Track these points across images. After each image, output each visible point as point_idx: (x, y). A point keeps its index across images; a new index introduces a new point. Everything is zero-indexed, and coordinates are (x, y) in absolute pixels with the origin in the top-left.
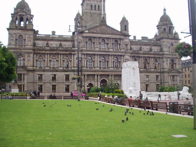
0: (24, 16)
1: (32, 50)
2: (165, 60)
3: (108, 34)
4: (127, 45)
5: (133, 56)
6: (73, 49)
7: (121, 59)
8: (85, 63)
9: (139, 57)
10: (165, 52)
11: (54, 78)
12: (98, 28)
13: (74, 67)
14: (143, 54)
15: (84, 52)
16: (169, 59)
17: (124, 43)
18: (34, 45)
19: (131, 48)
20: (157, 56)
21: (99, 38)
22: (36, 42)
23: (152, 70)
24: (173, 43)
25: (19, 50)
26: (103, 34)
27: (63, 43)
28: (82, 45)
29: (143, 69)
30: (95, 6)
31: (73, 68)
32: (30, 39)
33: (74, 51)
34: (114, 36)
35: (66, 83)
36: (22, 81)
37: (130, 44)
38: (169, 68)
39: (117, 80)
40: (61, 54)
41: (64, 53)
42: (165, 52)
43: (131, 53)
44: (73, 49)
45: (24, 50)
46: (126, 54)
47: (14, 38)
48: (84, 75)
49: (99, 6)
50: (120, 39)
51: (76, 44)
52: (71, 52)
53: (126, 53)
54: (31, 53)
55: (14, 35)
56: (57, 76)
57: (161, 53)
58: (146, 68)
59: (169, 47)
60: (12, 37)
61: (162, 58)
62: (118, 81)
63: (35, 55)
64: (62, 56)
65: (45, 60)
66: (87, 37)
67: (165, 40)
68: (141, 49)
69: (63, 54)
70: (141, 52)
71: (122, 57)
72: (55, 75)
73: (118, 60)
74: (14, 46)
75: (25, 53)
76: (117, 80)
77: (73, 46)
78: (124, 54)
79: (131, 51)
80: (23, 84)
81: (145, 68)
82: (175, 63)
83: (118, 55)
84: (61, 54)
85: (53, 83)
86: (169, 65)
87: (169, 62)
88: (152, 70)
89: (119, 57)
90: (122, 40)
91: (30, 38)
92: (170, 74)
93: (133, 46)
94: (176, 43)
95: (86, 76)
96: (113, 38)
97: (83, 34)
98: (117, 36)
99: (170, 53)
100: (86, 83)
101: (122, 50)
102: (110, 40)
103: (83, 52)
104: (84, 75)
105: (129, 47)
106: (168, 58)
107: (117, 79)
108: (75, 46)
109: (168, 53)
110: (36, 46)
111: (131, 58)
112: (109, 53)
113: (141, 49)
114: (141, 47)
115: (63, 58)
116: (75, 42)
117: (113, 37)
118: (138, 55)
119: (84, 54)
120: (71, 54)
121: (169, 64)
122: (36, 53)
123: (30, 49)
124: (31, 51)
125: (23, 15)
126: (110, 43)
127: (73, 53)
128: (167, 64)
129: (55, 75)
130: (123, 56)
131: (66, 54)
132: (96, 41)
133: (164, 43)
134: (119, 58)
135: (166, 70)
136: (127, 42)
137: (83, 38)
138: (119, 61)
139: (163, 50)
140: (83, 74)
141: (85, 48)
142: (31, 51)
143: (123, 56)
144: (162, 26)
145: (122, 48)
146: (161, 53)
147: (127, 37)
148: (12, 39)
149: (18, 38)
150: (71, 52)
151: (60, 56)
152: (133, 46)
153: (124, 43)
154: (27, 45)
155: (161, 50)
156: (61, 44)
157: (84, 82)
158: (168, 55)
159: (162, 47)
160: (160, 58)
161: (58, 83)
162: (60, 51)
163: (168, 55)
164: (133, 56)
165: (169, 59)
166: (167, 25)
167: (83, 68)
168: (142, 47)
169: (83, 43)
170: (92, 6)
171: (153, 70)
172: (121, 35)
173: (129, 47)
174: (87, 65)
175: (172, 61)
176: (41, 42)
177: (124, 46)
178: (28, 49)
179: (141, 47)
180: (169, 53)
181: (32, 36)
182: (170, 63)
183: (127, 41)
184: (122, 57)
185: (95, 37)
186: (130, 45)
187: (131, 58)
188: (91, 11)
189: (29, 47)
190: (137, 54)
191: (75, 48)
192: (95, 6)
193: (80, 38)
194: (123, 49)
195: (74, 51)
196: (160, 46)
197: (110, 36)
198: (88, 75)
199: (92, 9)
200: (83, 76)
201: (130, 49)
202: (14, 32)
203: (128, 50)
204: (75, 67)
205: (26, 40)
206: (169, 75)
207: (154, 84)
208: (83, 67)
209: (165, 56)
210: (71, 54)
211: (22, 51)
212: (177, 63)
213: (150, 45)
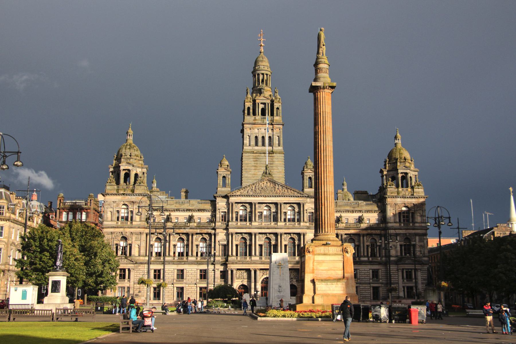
10: (390, 225)
11: (181, 274)
14: (346, 228)
20: (373, 232)
23: (362, 259)
30: (263, 138)
35: (200, 284)
36: (126, 280)
38: (399, 254)
49: (270, 137)
56: (185, 271)
72: (182, 271)
80: (128, 285)
85: (178, 284)
86: (399, 248)
87: (398, 244)
88: (362, 259)
92: (401, 267)
99: (402, 225)
112: (277, 230)
129: (182, 271)
153: (305, 212)
161: (186, 283)
163: (395, 229)
169: (231, 214)
171: (366, 259)
182: (401, 246)
188: (256, 148)
192: (263, 138)
199: (257, 144)
206: (398, 270)
207: (367, 286)
213: (360, 211)
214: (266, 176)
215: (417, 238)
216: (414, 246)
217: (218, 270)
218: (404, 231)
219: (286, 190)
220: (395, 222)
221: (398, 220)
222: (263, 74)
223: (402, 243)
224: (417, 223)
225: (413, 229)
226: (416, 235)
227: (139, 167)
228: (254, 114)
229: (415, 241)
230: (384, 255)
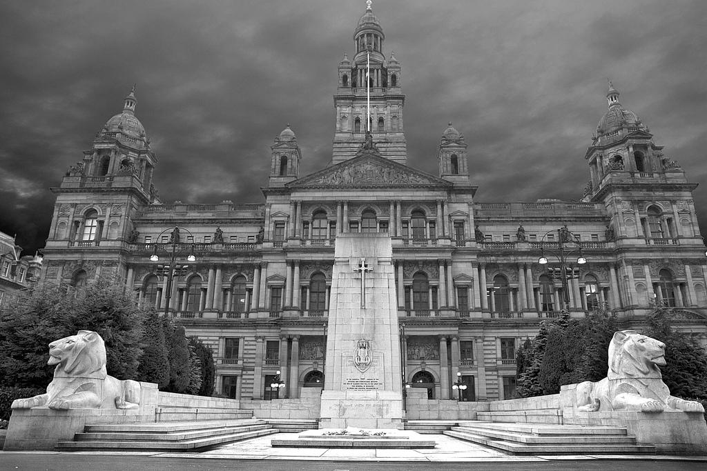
0: (113, 153)
1: (117, 256)
2: (628, 270)
3: (384, 188)
4: (460, 225)
5: (489, 267)
6: (259, 247)
7: (437, 277)
8: (296, 292)
9: (516, 266)
10: (626, 242)
12: (346, 172)
13: (258, 310)
15: (291, 256)
16: (647, 269)
17: (446, 218)
18: (133, 238)
19: (479, 236)
21: (352, 205)
22: (141, 230)
24: (659, 204)
25: (76, 257)
26: (364, 188)
27: (227, 230)
28: (288, 230)
29: (537, 310)
31: (252, 316)
32: (117, 219)
33: (259, 254)
34: (406, 196)
35: (223, 368)
37: (472, 217)
39: (422, 358)
40: (215, 267)
41: (225, 261)
42: (626, 242)
43: (480, 254)
44: (259, 247)
45: (92, 256)
46: (458, 258)
47: (71, 219)
48: (290, 341)
50: (433, 204)
51: (269, 228)
52: (250, 260)
53: (455, 252)
54: (111, 264)
55: (72, 210)
57: (611, 245)
58: (551, 309)
59: (643, 220)
60: (63, 215)
61: (617, 266)
62: (428, 362)
63: (131, 271)
64: (218, 271)
65: (162, 289)
66: (305, 205)
67: (617, 195)
68: (521, 236)
69: (224, 268)
70: (524, 247)
71: (442, 268)
73: (428, 282)
74: (65, 244)
75: (98, 263)
76: (422, 358)
77: (258, 237)
78: (447, 256)
79: (479, 246)
81: (545, 309)
82: (682, 285)
83: (426, 263)
84: (215, 267)
87: (649, 281)
89: (428, 271)
90: (439, 207)
91: (115, 215)
93: (486, 229)
94: (673, 202)
95: (295, 344)
96: (404, 204)
97: (293, 195)
98: (418, 193)
99: (652, 242)
100: (294, 370)
101: (441, 242)
102: (392, 207)
103: (289, 255)
104: (290, 341)
105: (470, 230)
106: (645, 262)
107: (422, 354)
108: (266, 236)
109: (642, 242)
110: (140, 241)
111: (483, 271)
113: (521, 236)
114: (521, 230)
115: (223, 280)
116: (267, 222)
117: (403, 198)
118: (512, 259)
119: (292, 264)
120: (251, 267)
121: (650, 286)
122: (134, 267)
123: (110, 251)
124: (115, 257)
125: (109, 150)
126: (392, 218)
127: (258, 261)
128: (640, 286)
130: (446, 264)
131: (234, 267)
132: (339, 214)
133: (619, 206)
134: (429, 274)
135: (637, 312)
136: (463, 214)
137: (292, 207)
138: (433, 283)
139: (619, 234)
140: (284, 336)
141: (298, 242)
142: (115, 257)
143: (446, 264)
144: (604, 148)
145: (441, 234)
146: (611, 245)
147: (464, 196)
148: (63, 223)
149: (80, 219)
150: (250, 260)
151: (211, 271)
152: (486, 229)
153: (446, 218)
154: (106, 240)
155: (611, 235)
156: (219, 237)
157: (289, 365)
158: (640, 250)
159: (612, 222)
160: (606, 266)
162: (214, 254)
164: (489, 267)
165: (647, 269)
166: (623, 141)
167: (287, 314)
168: (526, 228)
169: (292, 225)
170: (358, 121)
172: (431, 189)
173: (470, 230)
174: (304, 302)
175: (665, 271)
176: (159, 230)
177: (450, 230)
178: (107, 253)
179: (521, 230)
180: (648, 240)
181: (123, 212)
182: (655, 285)
183: (463, 208)
184: (442, 268)
185: (334, 204)
186: (472, 224)
187: (483, 271)
189: (109, 244)
190: (506, 254)
191: (266, 245)
193: (287, 209)
194: (444, 237)
195: (259, 254)
196: (605, 220)
197: (392, 194)
198: (303, 340)
200: (285, 344)
201: (473, 237)
202: (72, 202)
203: (468, 244)
204: (263, 310)
205: (105, 224)
208: (285, 309)
209: (629, 256)
210: (251, 267)
211: (88, 257)
212: (691, 282)
213: (557, 220)
214: (367, 151)
215: (687, 267)
216: (682, 285)
217: (264, 338)
218: (658, 254)
219: (404, 176)
220: (639, 238)
221: (641, 233)
222: (369, 35)
223: (657, 280)
224: (682, 237)
225: (678, 250)
226: (685, 261)
227: (133, 150)
228: (354, 85)
229: (685, 275)
230: (618, 306)
